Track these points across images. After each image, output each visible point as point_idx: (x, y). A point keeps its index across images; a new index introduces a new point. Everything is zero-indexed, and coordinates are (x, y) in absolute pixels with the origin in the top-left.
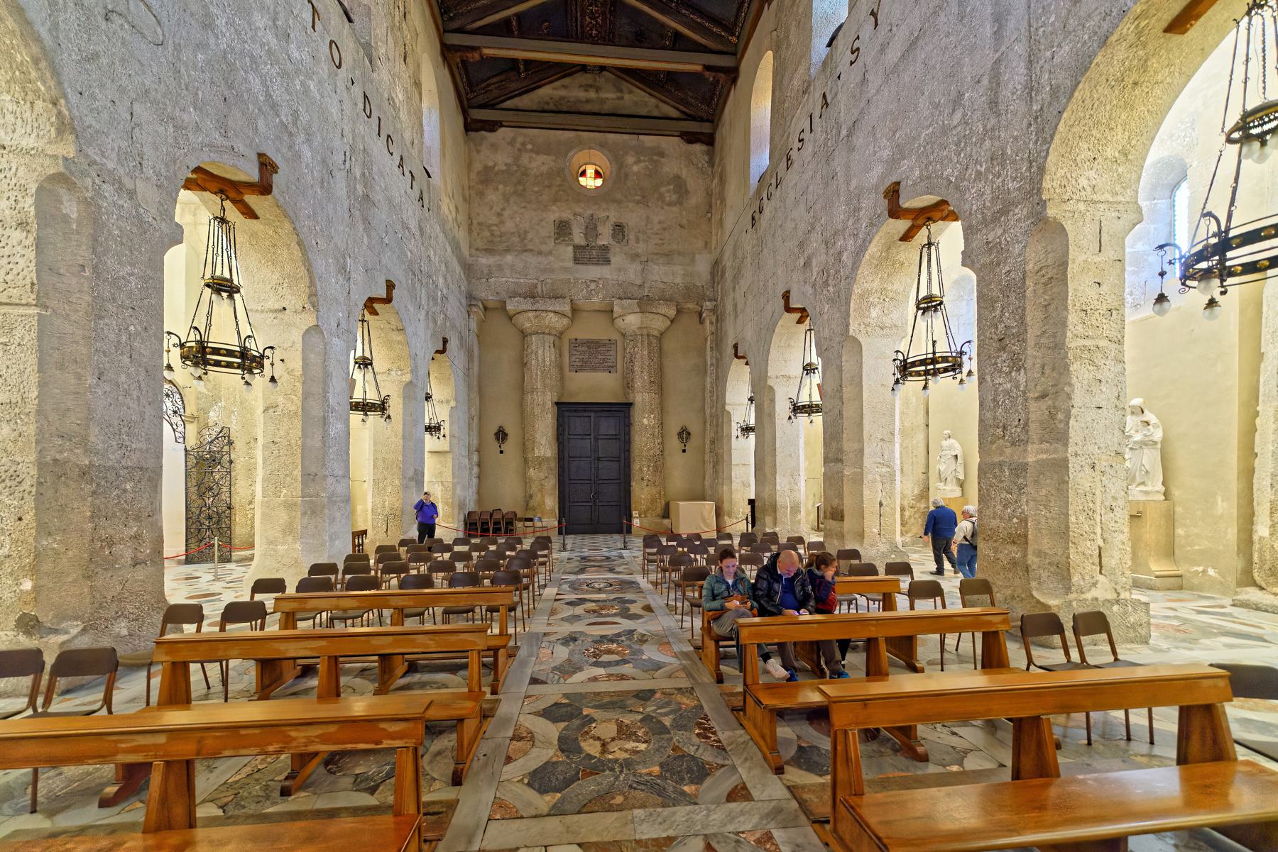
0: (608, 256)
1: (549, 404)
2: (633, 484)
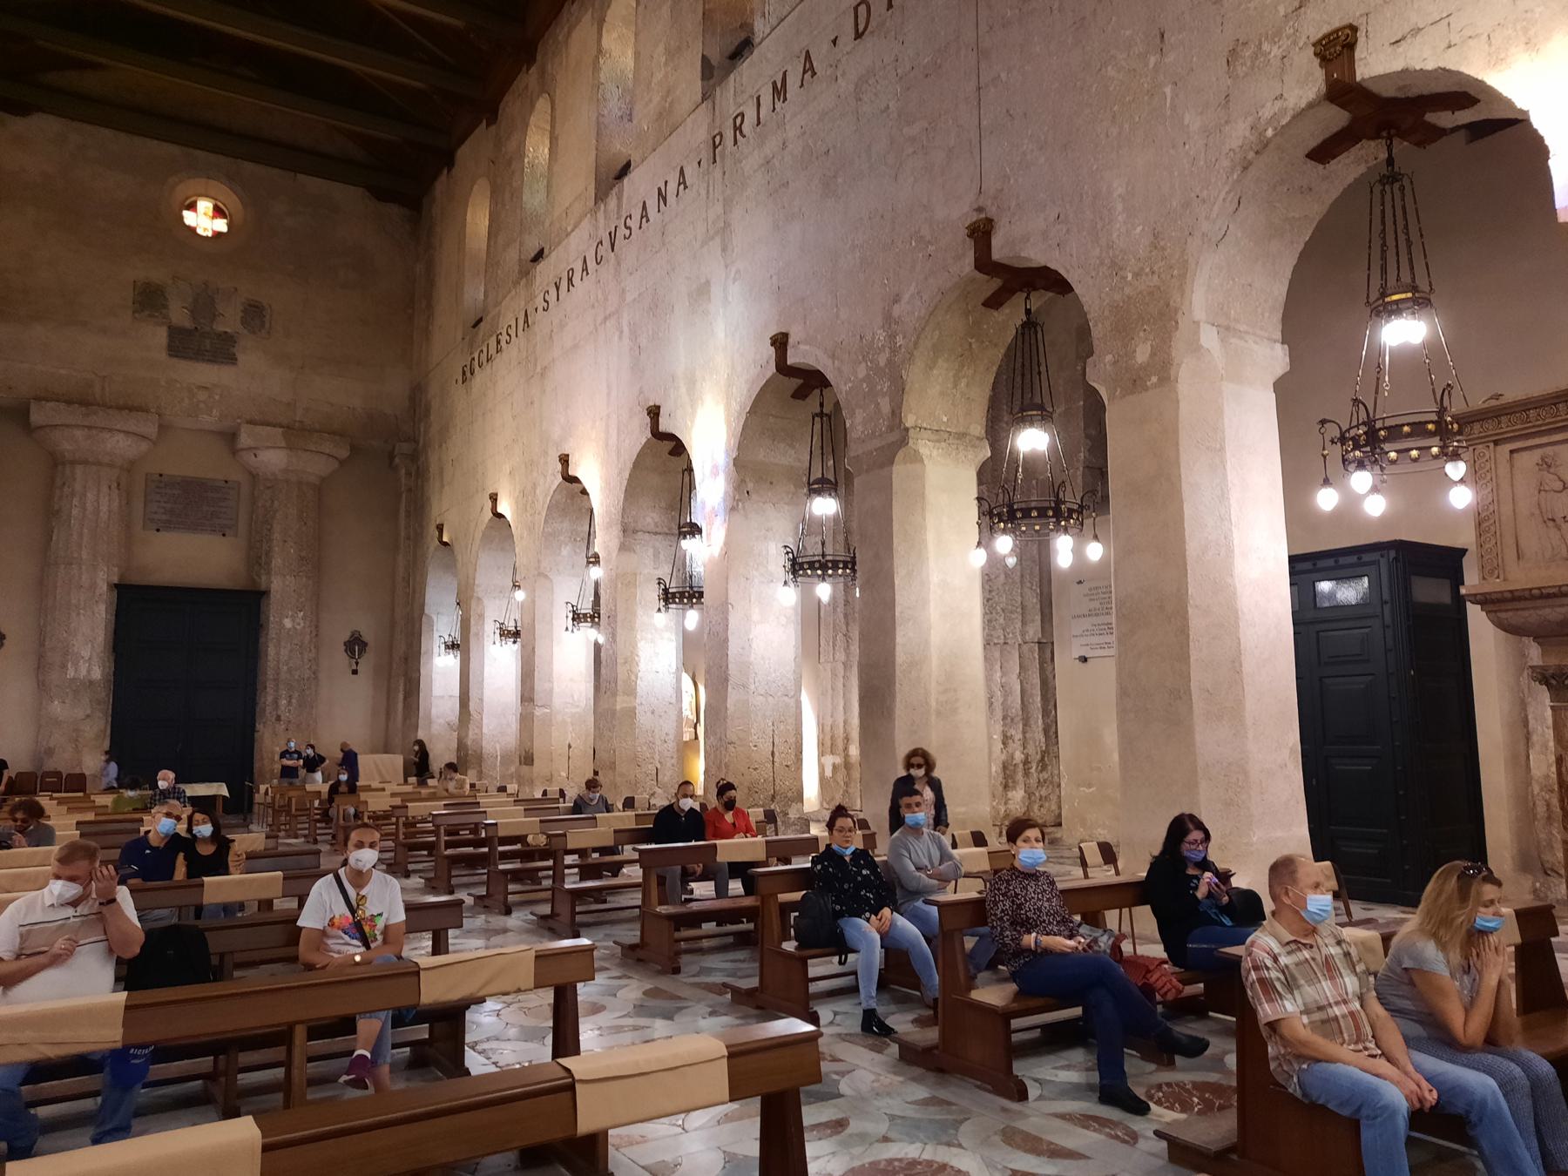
0: (235, 350)
1: (103, 587)
2: (259, 726)
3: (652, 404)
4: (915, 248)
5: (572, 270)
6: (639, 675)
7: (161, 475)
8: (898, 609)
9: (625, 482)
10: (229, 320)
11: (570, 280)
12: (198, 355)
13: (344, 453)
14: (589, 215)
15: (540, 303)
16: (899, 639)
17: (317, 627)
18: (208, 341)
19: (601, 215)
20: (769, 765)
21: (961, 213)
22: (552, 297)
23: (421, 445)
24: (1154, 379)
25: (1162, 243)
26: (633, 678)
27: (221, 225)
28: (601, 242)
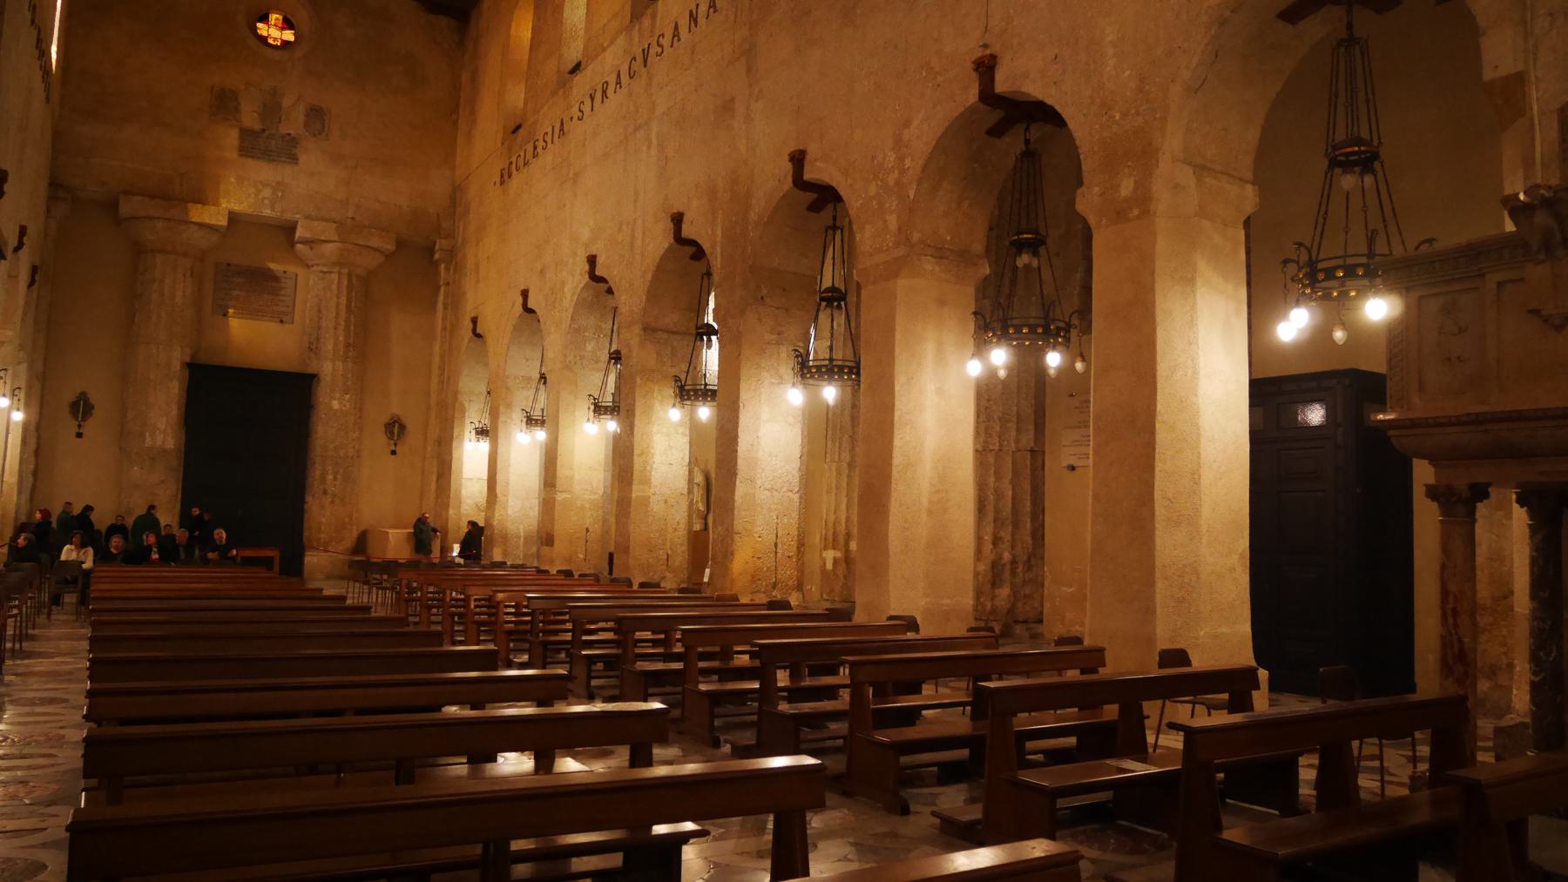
1: (177, 365)
2: (309, 498)
3: (675, 211)
4: (925, 77)
5: (607, 82)
6: (654, 466)
7: (229, 265)
8: (897, 414)
9: (648, 284)
10: (294, 124)
11: (604, 92)
12: (267, 155)
13: (390, 247)
14: (624, 33)
15: (577, 114)
16: (897, 442)
17: (361, 410)
18: (274, 142)
19: (635, 33)
20: (772, 555)
21: (969, 49)
22: (587, 108)
23: (460, 240)
24: (1136, 212)
25: (1147, 87)
26: (648, 468)
27: (289, 36)
28: (634, 58)
